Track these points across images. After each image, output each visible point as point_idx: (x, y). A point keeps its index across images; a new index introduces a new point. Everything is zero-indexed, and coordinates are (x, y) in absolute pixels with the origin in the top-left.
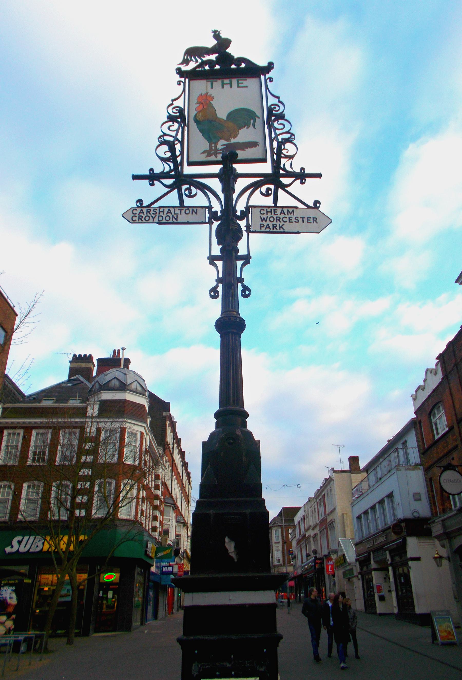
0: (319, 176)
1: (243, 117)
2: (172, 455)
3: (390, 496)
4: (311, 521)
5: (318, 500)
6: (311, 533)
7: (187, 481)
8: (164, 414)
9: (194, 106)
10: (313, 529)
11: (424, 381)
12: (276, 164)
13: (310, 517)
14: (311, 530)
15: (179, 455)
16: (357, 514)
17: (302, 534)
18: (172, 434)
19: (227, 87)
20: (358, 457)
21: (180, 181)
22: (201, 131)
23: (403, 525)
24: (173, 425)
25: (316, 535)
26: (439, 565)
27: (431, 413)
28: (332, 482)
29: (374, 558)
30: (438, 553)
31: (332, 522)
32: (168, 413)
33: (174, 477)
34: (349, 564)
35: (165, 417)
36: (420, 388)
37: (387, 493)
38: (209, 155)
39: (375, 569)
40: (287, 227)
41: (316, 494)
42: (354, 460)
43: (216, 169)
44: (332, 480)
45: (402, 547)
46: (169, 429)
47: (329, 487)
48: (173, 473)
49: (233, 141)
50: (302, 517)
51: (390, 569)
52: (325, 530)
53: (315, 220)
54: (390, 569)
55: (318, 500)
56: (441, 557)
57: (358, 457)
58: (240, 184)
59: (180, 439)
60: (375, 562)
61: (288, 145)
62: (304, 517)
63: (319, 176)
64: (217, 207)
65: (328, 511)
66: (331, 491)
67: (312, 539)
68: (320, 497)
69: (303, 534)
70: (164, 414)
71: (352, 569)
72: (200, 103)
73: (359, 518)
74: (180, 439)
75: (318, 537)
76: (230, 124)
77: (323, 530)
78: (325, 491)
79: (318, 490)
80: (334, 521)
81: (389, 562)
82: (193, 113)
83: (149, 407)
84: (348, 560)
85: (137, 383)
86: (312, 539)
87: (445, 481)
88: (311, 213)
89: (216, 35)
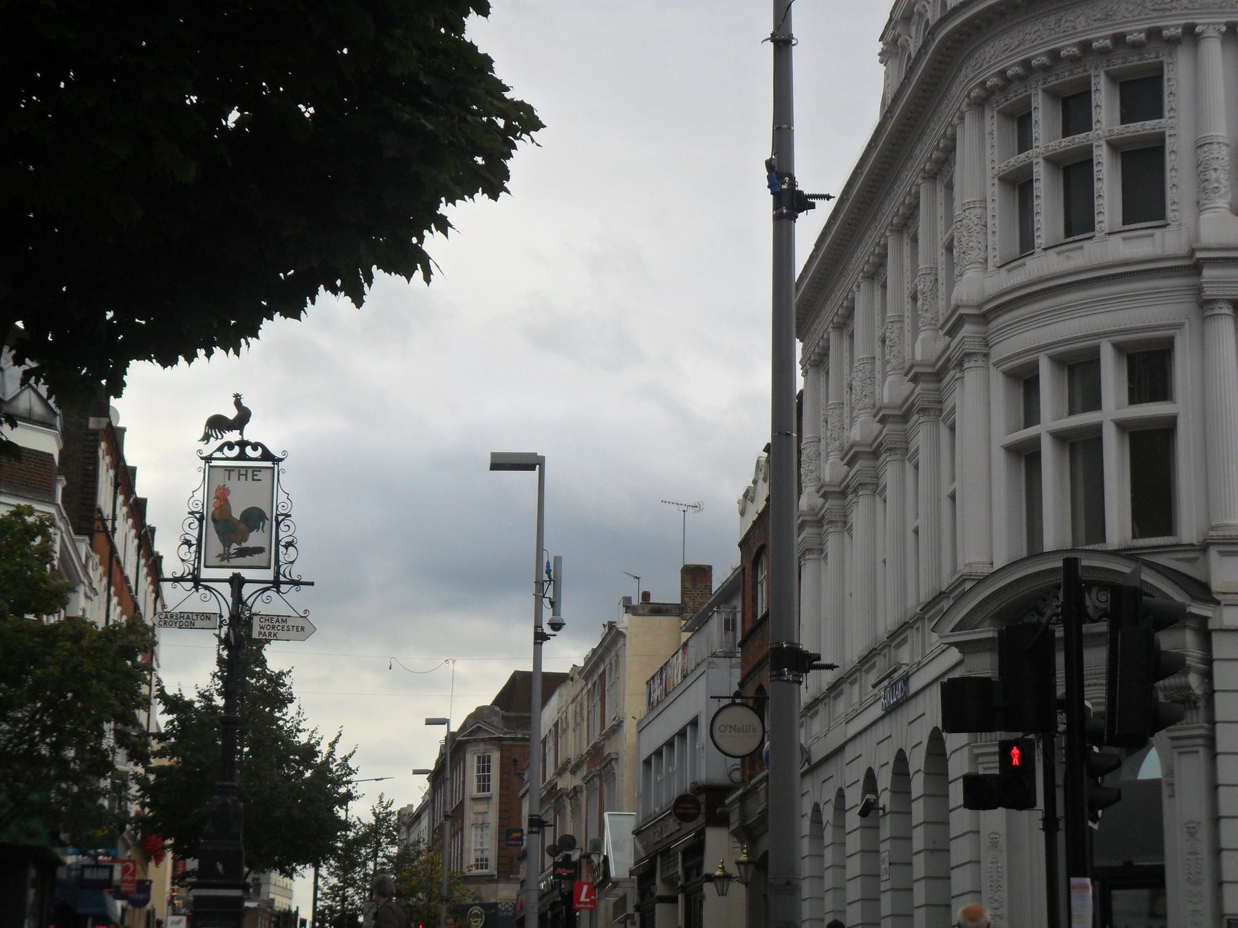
0: (312, 584)
1: (254, 518)
2: (109, 536)
3: (694, 723)
4: (574, 746)
5: (590, 685)
6: (567, 782)
7: (151, 588)
8: (93, 423)
9: (213, 501)
10: (573, 772)
11: (755, 482)
12: (277, 573)
13: (570, 731)
14: (568, 776)
15: (130, 521)
16: (644, 756)
17: (548, 779)
18: (112, 472)
19: (243, 478)
20: (710, 568)
21: (197, 581)
22: (218, 532)
23: (702, 798)
24: (115, 437)
25: (576, 791)
26: (722, 893)
27: (756, 562)
28: (620, 644)
29: (662, 872)
30: (723, 868)
31: (611, 761)
32: (104, 420)
33: (115, 600)
34: (616, 884)
35: (95, 433)
36: (748, 496)
37: (690, 717)
38: (223, 560)
39: (662, 899)
40: (280, 634)
41: (588, 660)
42: (696, 575)
43: (227, 573)
44: (621, 635)
45: (696, 850)
46: (104, 461)
47: (613, 654)
48: (113, 589)
49: (244, 545)
50: (551, 726)
51: (681, 897)
52: (597, 780)
53: (303, 629)
54: (681, 897)
55: (590, 685)
56: (727, 877)
57: (710, 568)
58: (247, 590)
59: (134, 470)
60: (663, 880)
61: (291, 548)
62: (556, 725)
63: (312, 584)
64: (226, 615)
65: (608, 725)
66: (617, 662)
67: (567, 802)
68: (596, 677)
69: (550, 781)
70: (93, 423)
71: (623, 899)
72: (217, 497)
73: (647, 762)
74: (134, 470)
75: (583, 797)
76: (242, 526)
77: (592, 778)
78: (607, 662)
79: (594, 651)
80: (617, 759)
81: (680, 883)
82: (212, 509)
83: (61, 452)
84: (613, 874)
85: (33, 395)
86: (567, 802)
87: (723, 728)
88: (301, 623)
89: (238, 403)
